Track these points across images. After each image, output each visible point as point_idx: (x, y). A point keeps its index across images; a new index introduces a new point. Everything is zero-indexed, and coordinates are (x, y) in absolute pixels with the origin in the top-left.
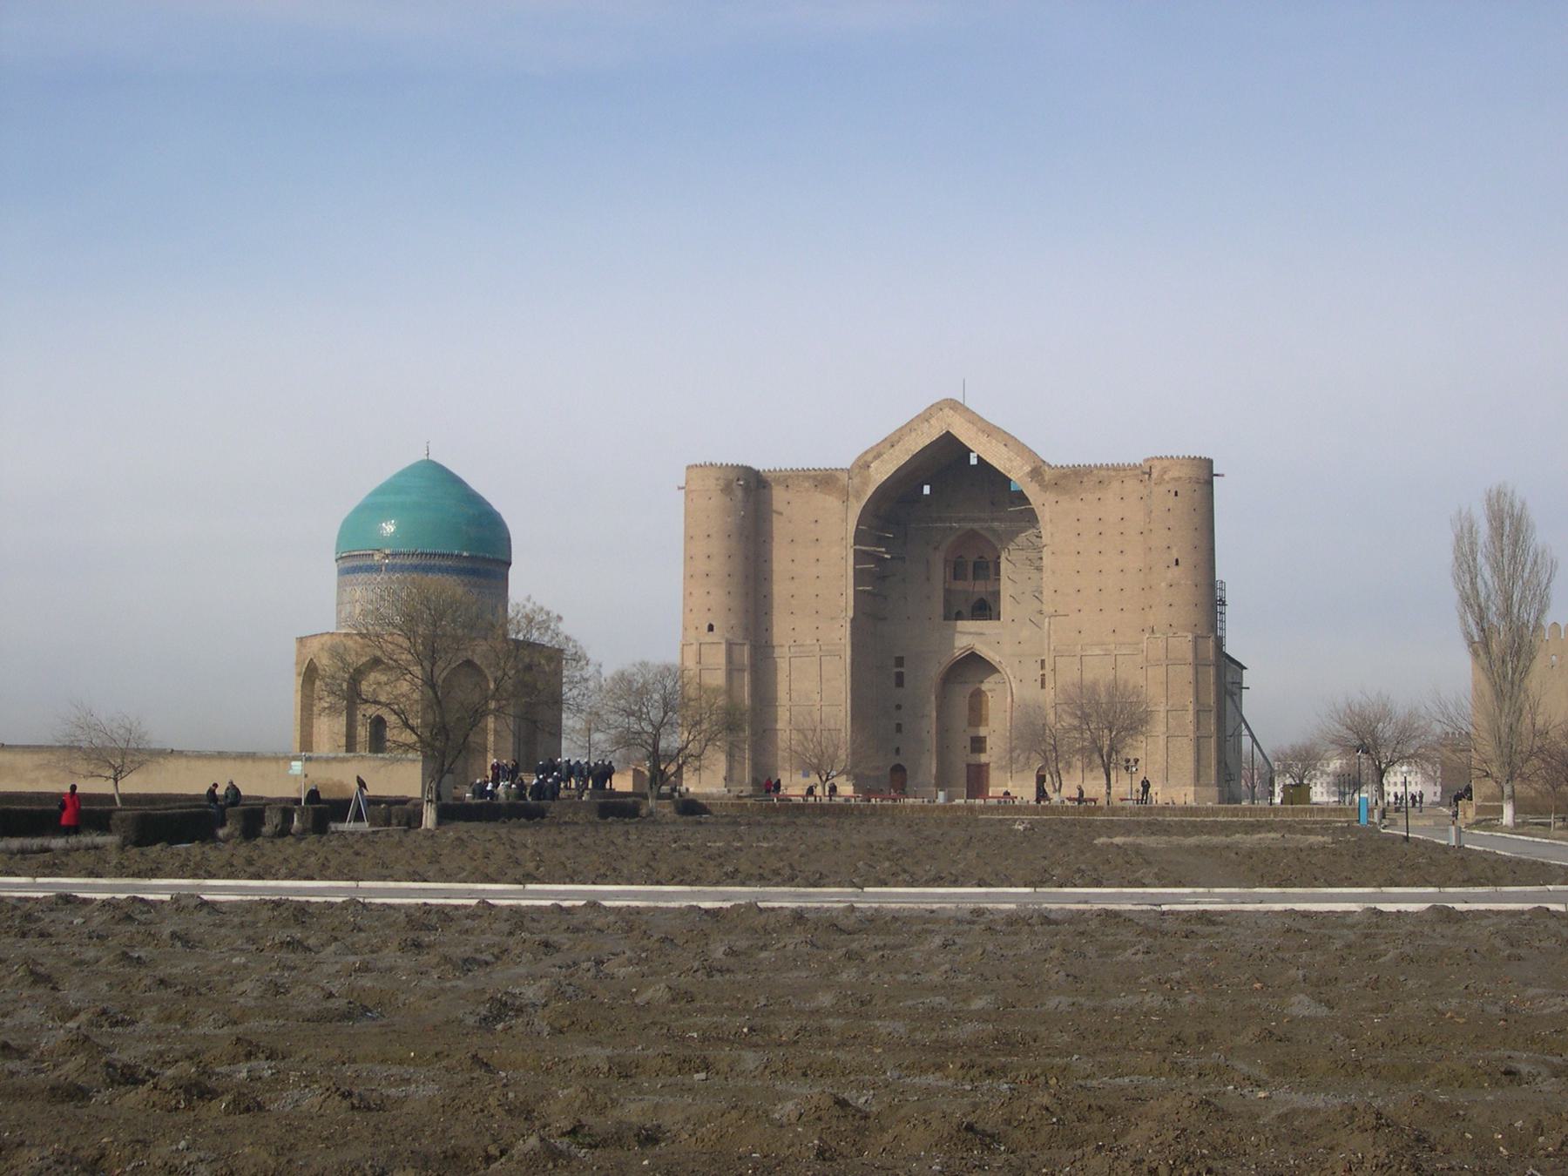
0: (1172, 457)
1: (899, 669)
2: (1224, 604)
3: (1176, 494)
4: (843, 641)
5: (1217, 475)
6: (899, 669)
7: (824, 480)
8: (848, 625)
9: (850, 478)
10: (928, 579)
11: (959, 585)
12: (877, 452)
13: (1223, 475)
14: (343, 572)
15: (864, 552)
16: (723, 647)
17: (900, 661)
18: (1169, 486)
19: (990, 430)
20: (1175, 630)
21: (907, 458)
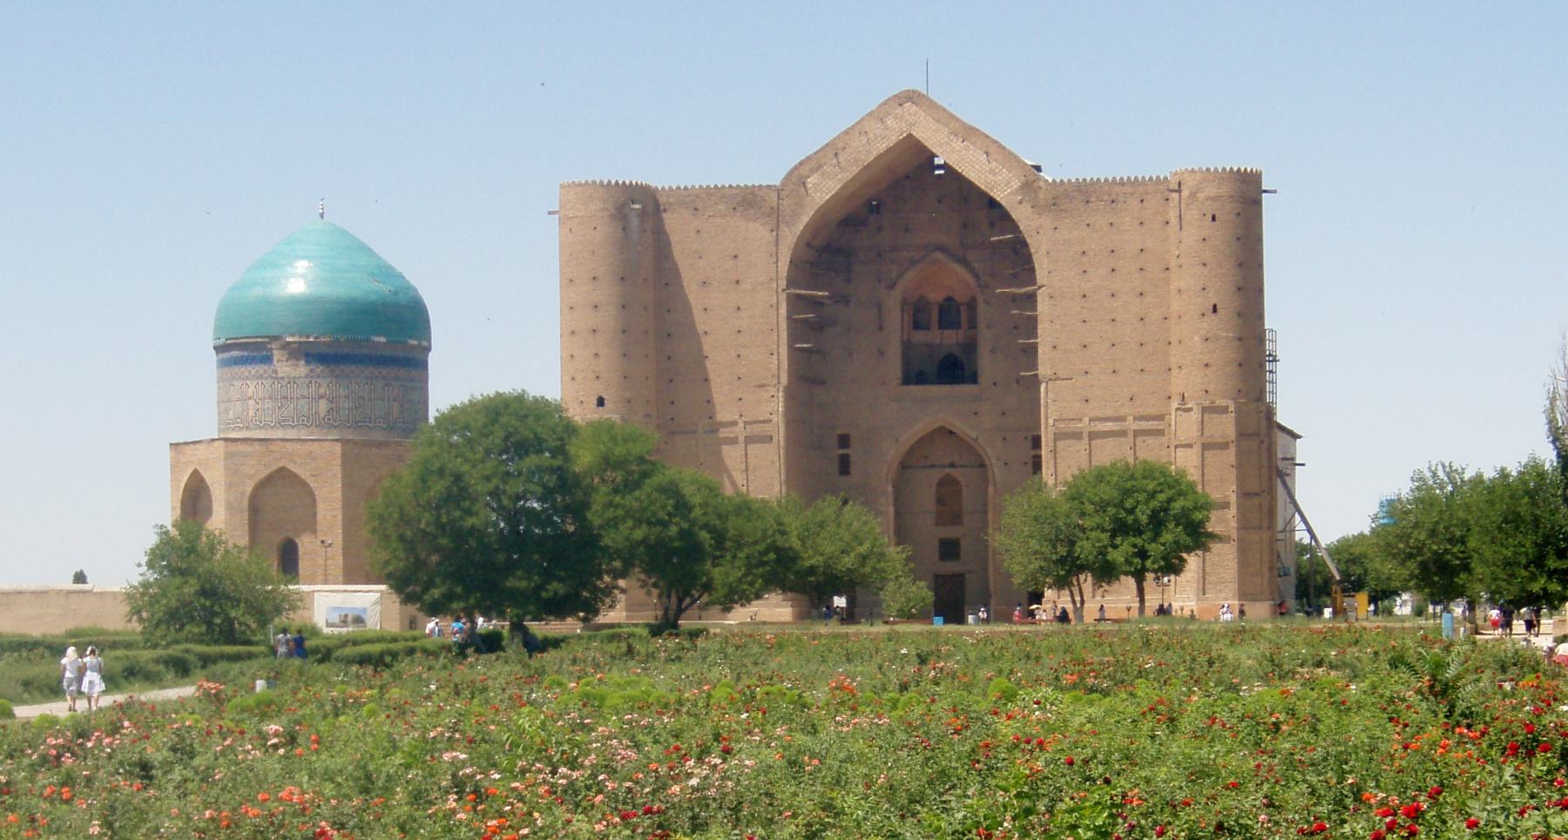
0: (1208, 170)
1: (841, 452)
2: (1275, 360)
3: (1214, 218)
5: (1265, 191)
6: (841, 452)
7: (747, 200)
9: (779, 199)
10: (880, 328)
11: (920, 337)
12: (813, 164)
13: (1275, 192)
14: (224, 364)
15: (799, 297)
17: (844, 441)
19: (969, 133)
20: (1211, 397)
21: (855, 170)
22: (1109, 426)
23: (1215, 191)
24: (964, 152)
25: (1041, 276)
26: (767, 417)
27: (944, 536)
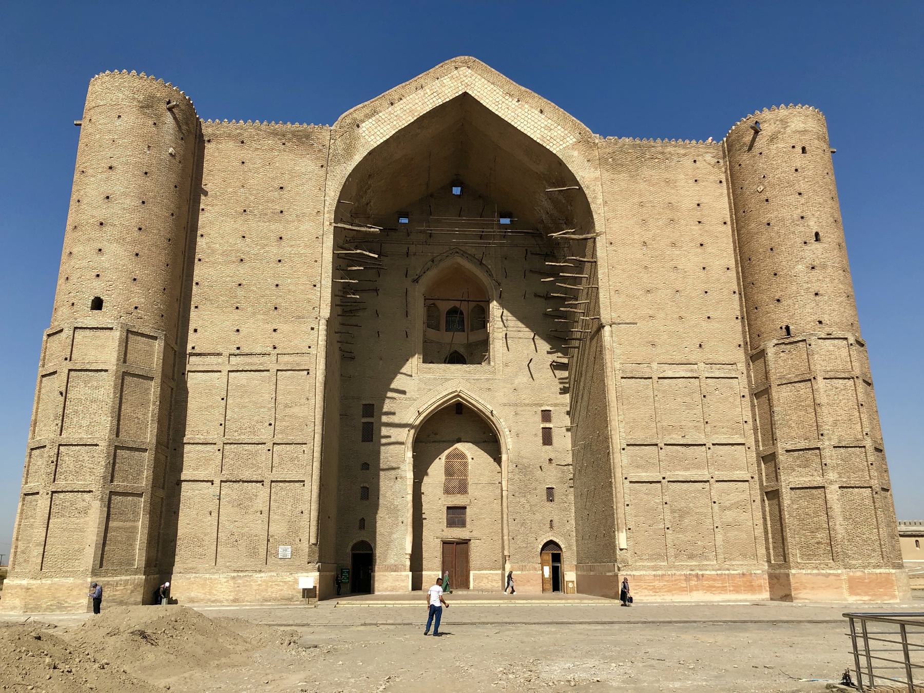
4: (313, 351)
8: (323, 327)
11: (432, 333)
16: (117, 334)
18: (793, 142)
20: (827, 330)
22: (681, 371)
23: (802, 125)
24: (520, 110)
25: (599, 226)
26: (306, 350)
27: (451, 504)
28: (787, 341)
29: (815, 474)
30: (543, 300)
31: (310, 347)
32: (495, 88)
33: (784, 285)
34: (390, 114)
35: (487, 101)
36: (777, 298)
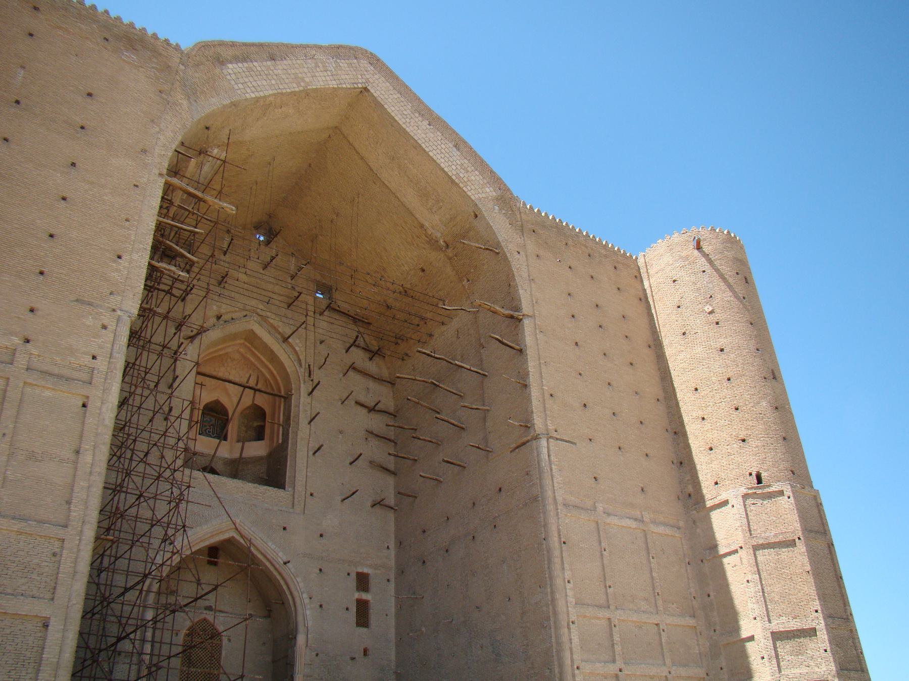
4: (101, 364)
28: (759, 491)
29: (812, 663)
30: (365, 411)
31: (94, 357)
32: (402, 99)
33: (751, 423)
34: (268, 68)
35: (393, 109)
36: (742, 437)
